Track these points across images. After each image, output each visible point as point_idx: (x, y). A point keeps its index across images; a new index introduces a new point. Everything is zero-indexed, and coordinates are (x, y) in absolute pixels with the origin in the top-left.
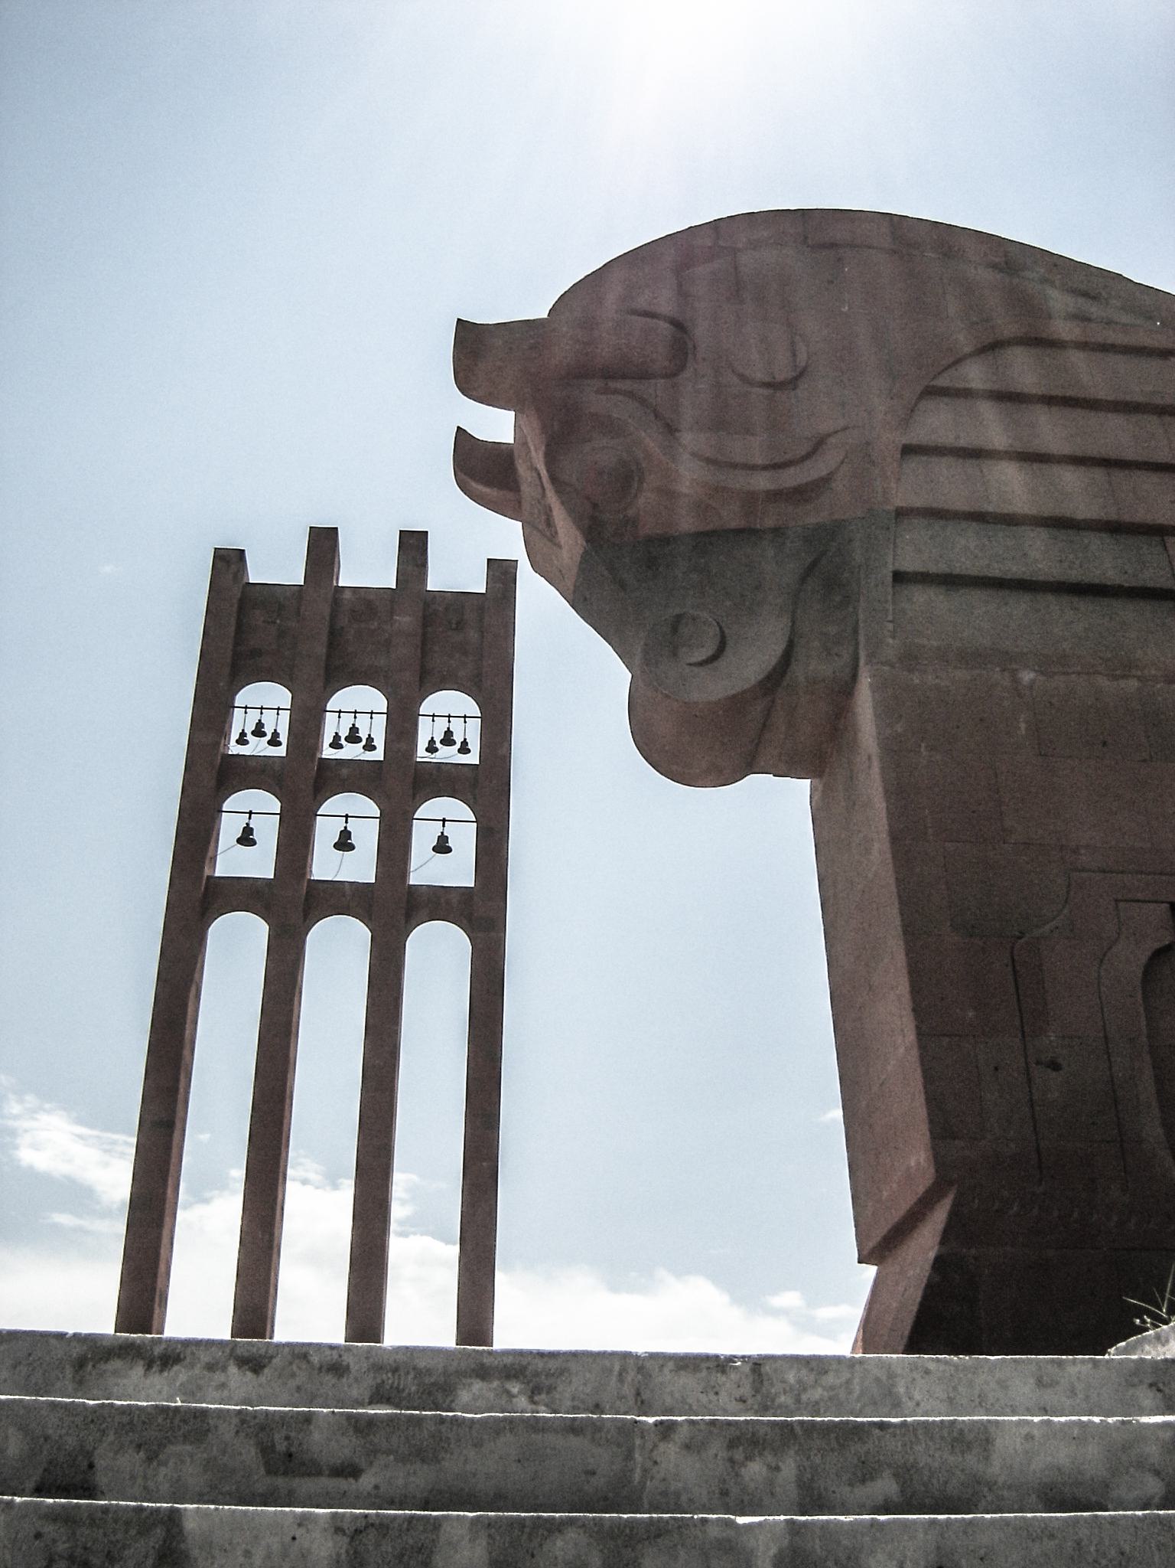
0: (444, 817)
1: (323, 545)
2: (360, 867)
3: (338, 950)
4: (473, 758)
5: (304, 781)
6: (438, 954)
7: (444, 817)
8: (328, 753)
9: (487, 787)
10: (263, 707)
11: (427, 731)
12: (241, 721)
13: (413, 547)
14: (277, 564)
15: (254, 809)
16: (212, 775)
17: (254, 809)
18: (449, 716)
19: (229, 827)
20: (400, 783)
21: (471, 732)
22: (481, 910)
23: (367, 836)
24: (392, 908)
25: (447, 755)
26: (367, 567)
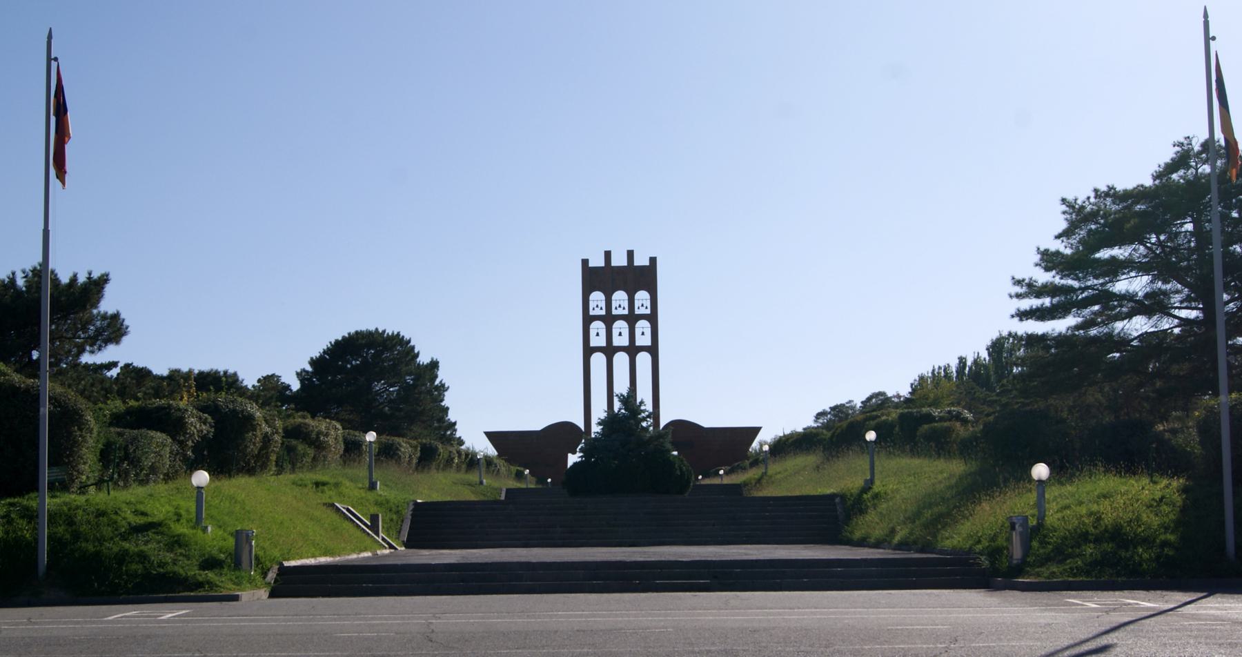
0: (643, 326)
1: (608, 255)
2: (623, 341)
3: (621, 360)
4: (648, 312)
5: (609, 319)
6: (644, 359)
7: (643, 326)
8: (614, 312)
9: (653, 318)
10: (597, 298)
11: (637, 304)
12: (592, 305)
13: (630, 254)
14: (597, 261)
15: (598, 327)
16: (588, 319)
17: (598, 327)
18: (642, 297)
19: (592, 333)
20: (632, 319)
21: (648, 303)
22: (653, 350)
23: (626, 333)
24: (632, 350)
25: (643, 311)
26: (619, 260)
